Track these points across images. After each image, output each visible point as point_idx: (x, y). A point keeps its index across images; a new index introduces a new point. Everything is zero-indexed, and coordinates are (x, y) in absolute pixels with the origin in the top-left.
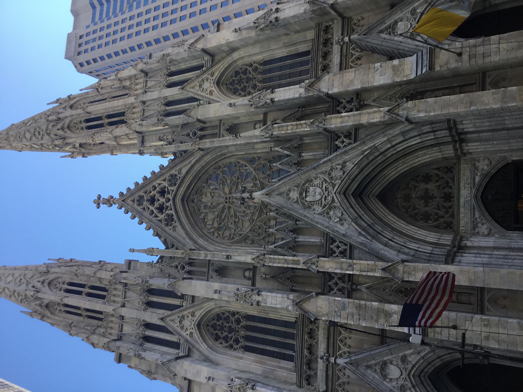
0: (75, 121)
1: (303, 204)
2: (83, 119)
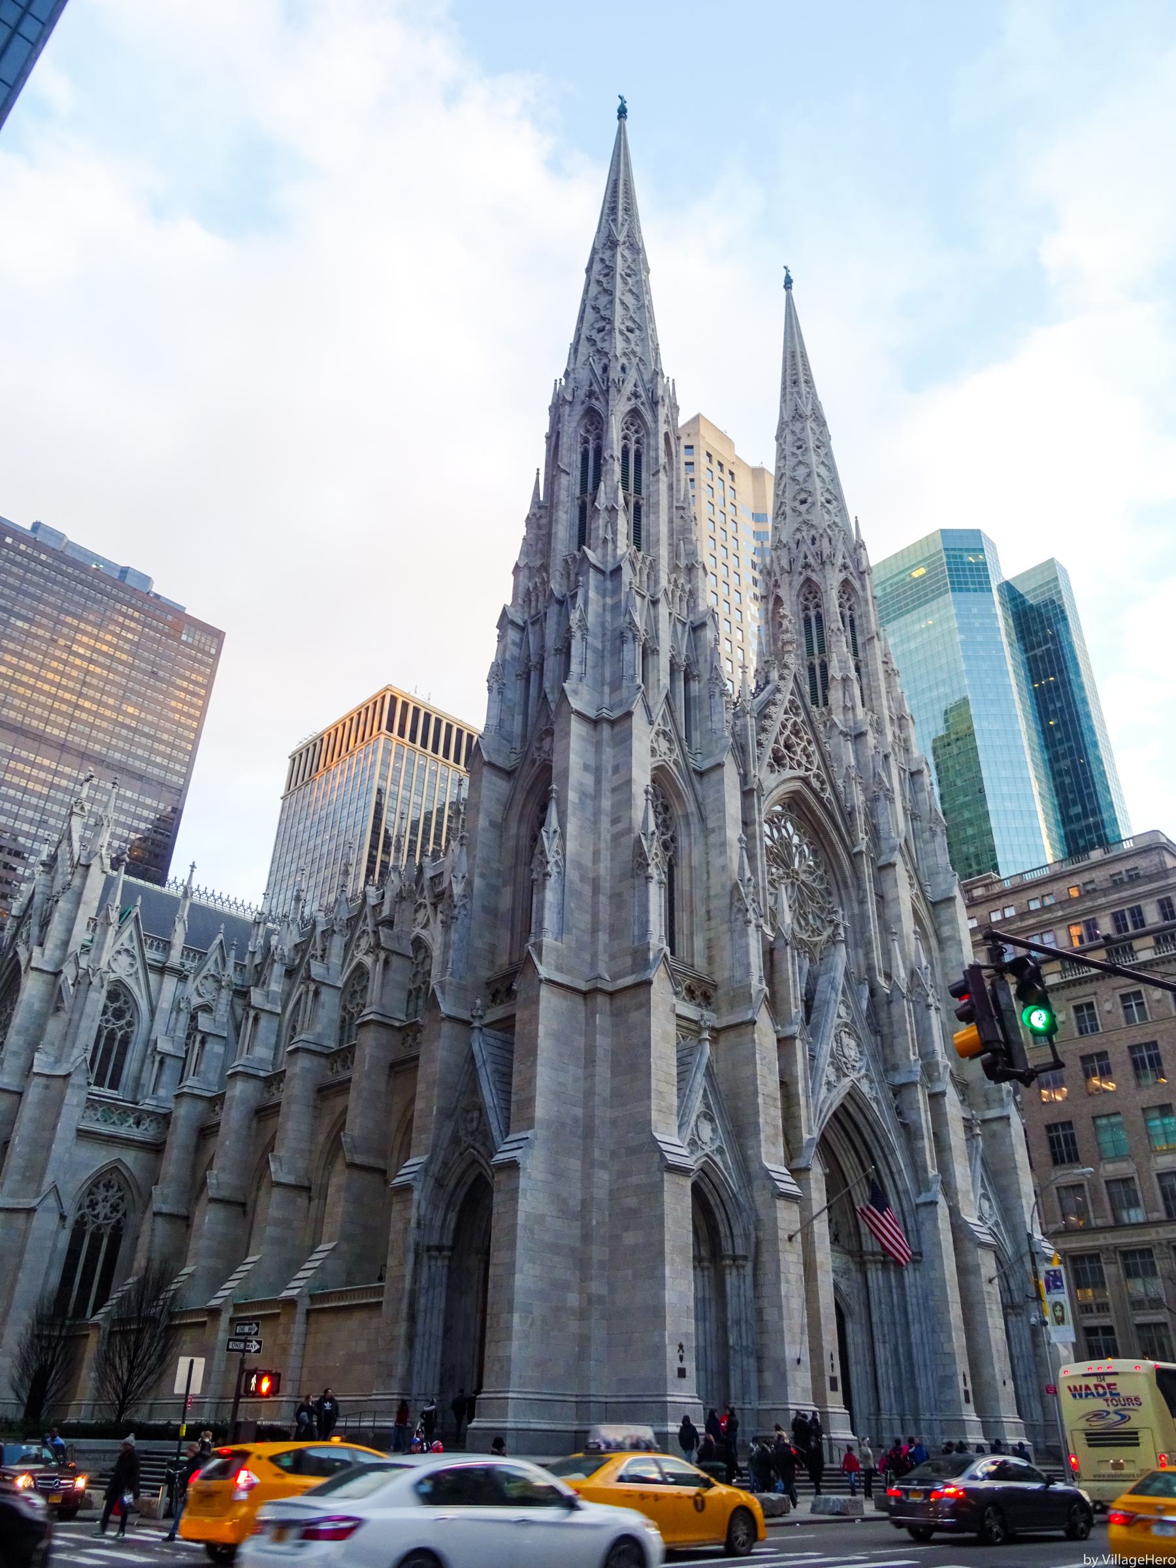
0: (853, 599)
2: (856, 616)
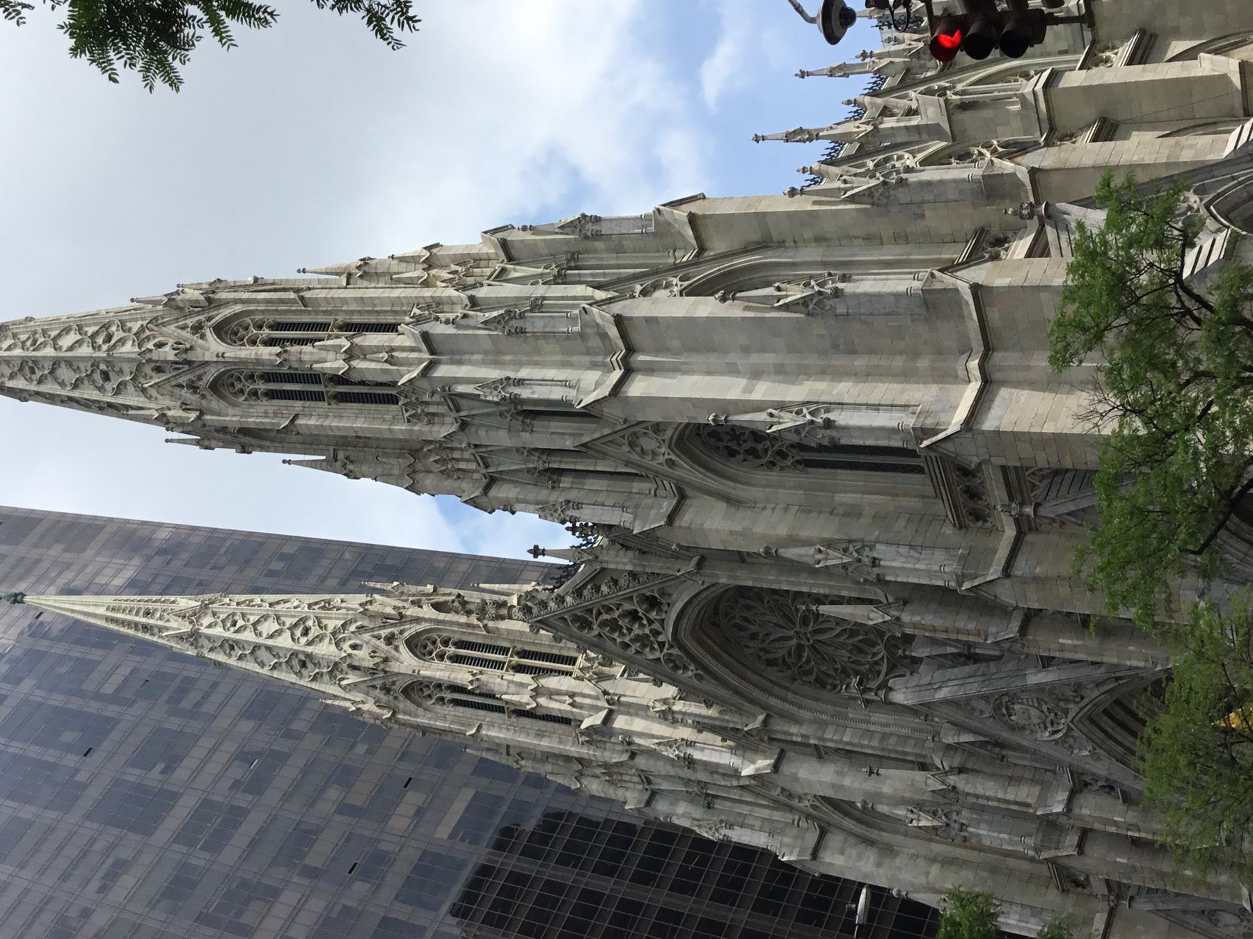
1: (1006, 723)
